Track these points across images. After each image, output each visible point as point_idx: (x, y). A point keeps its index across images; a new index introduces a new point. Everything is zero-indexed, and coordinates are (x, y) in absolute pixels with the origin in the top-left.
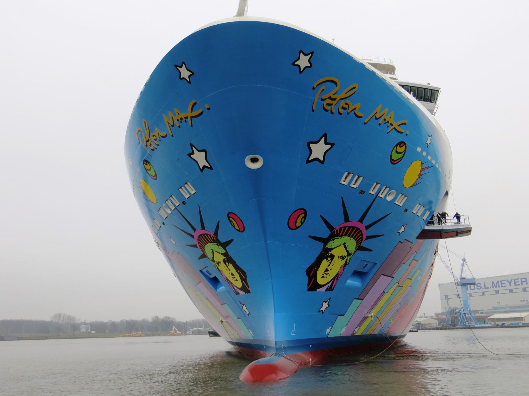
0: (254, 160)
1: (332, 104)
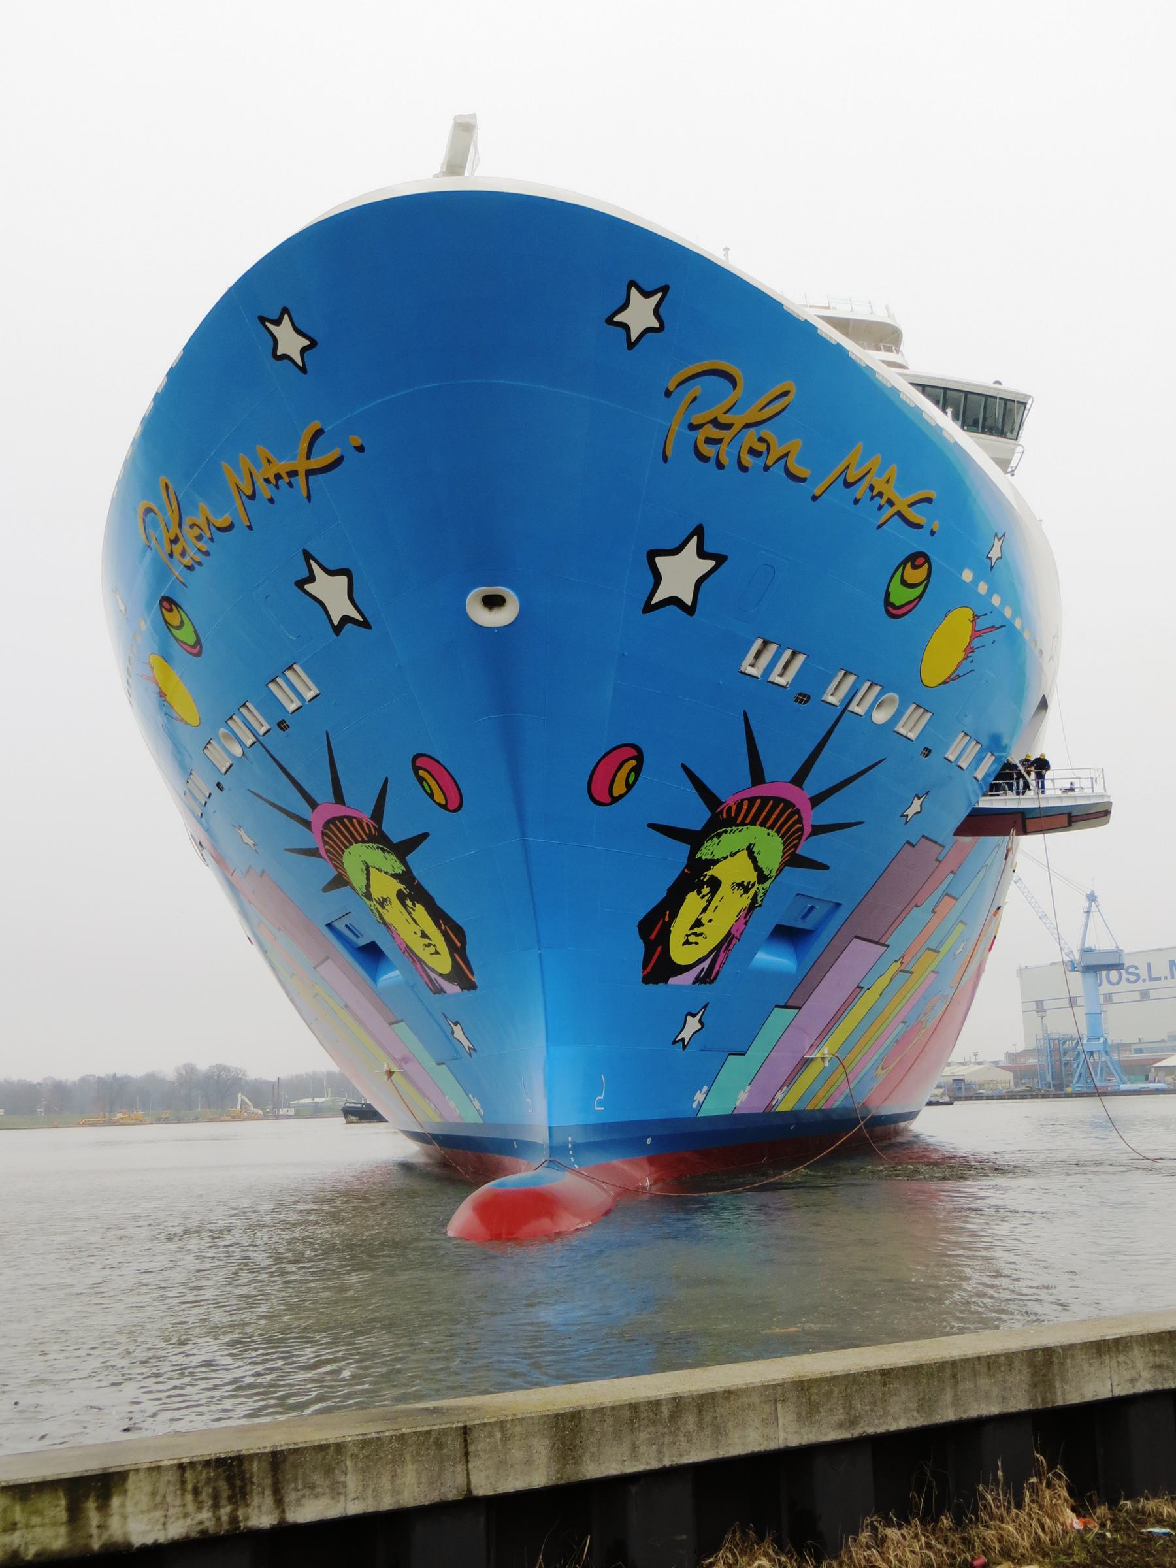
0: (493, 602)
1: (719, 441)
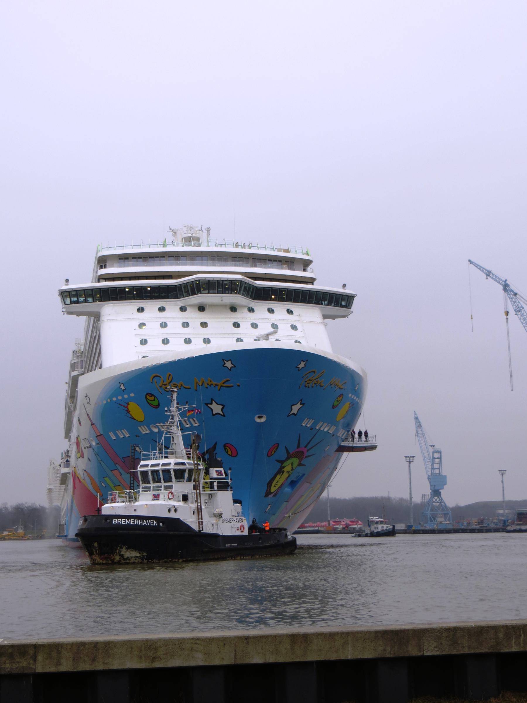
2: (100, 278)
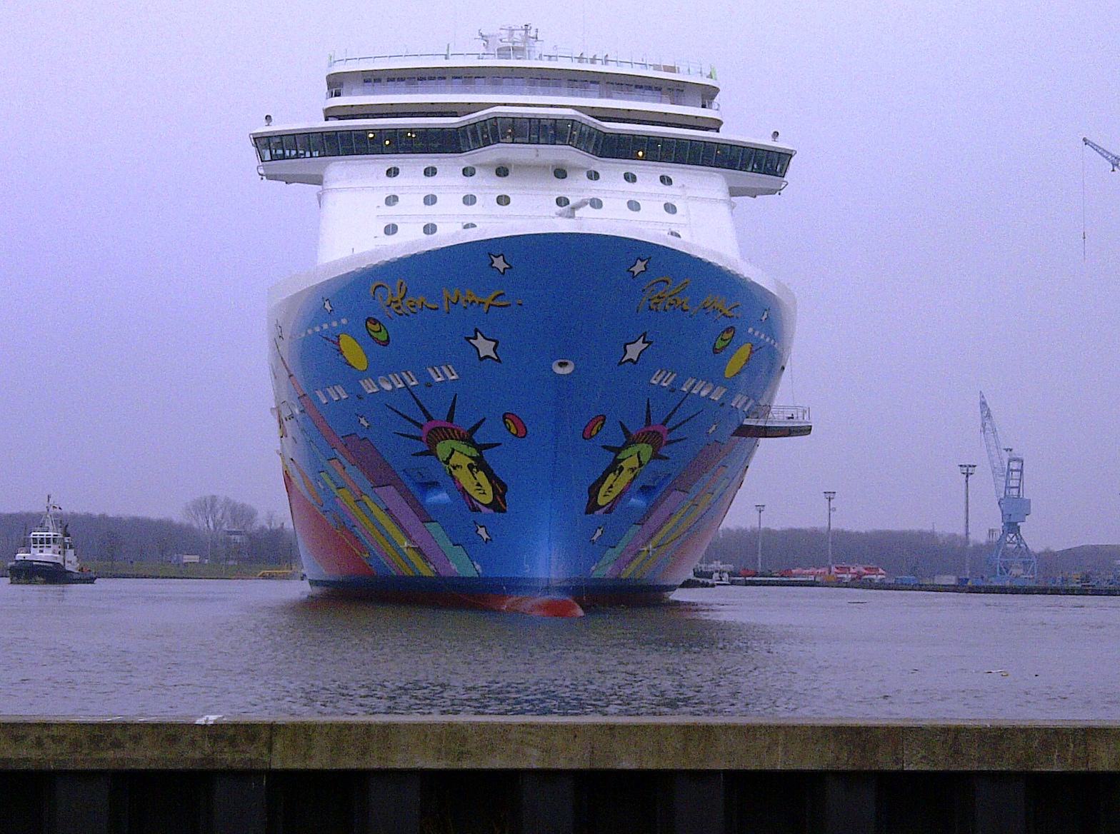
0: (562, 365)
2: (329, 114)
